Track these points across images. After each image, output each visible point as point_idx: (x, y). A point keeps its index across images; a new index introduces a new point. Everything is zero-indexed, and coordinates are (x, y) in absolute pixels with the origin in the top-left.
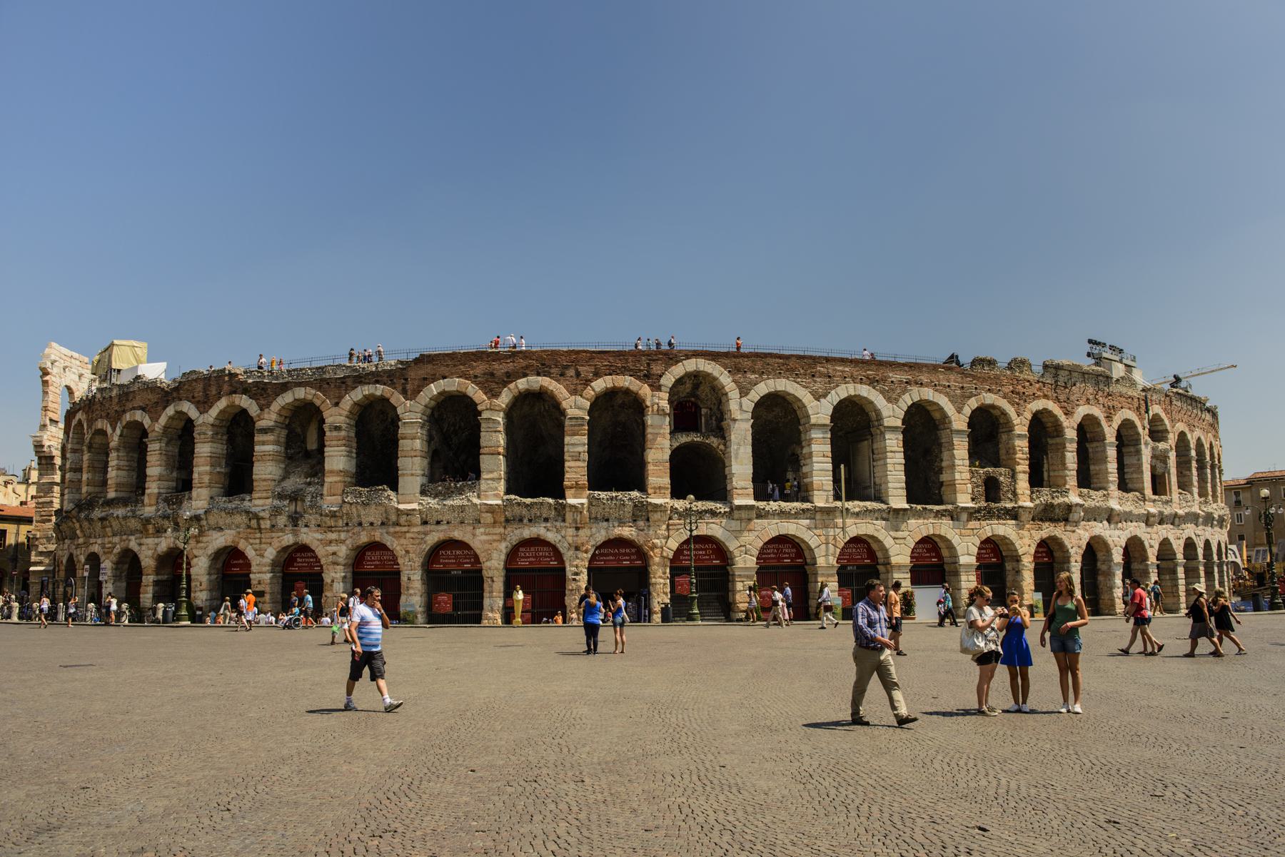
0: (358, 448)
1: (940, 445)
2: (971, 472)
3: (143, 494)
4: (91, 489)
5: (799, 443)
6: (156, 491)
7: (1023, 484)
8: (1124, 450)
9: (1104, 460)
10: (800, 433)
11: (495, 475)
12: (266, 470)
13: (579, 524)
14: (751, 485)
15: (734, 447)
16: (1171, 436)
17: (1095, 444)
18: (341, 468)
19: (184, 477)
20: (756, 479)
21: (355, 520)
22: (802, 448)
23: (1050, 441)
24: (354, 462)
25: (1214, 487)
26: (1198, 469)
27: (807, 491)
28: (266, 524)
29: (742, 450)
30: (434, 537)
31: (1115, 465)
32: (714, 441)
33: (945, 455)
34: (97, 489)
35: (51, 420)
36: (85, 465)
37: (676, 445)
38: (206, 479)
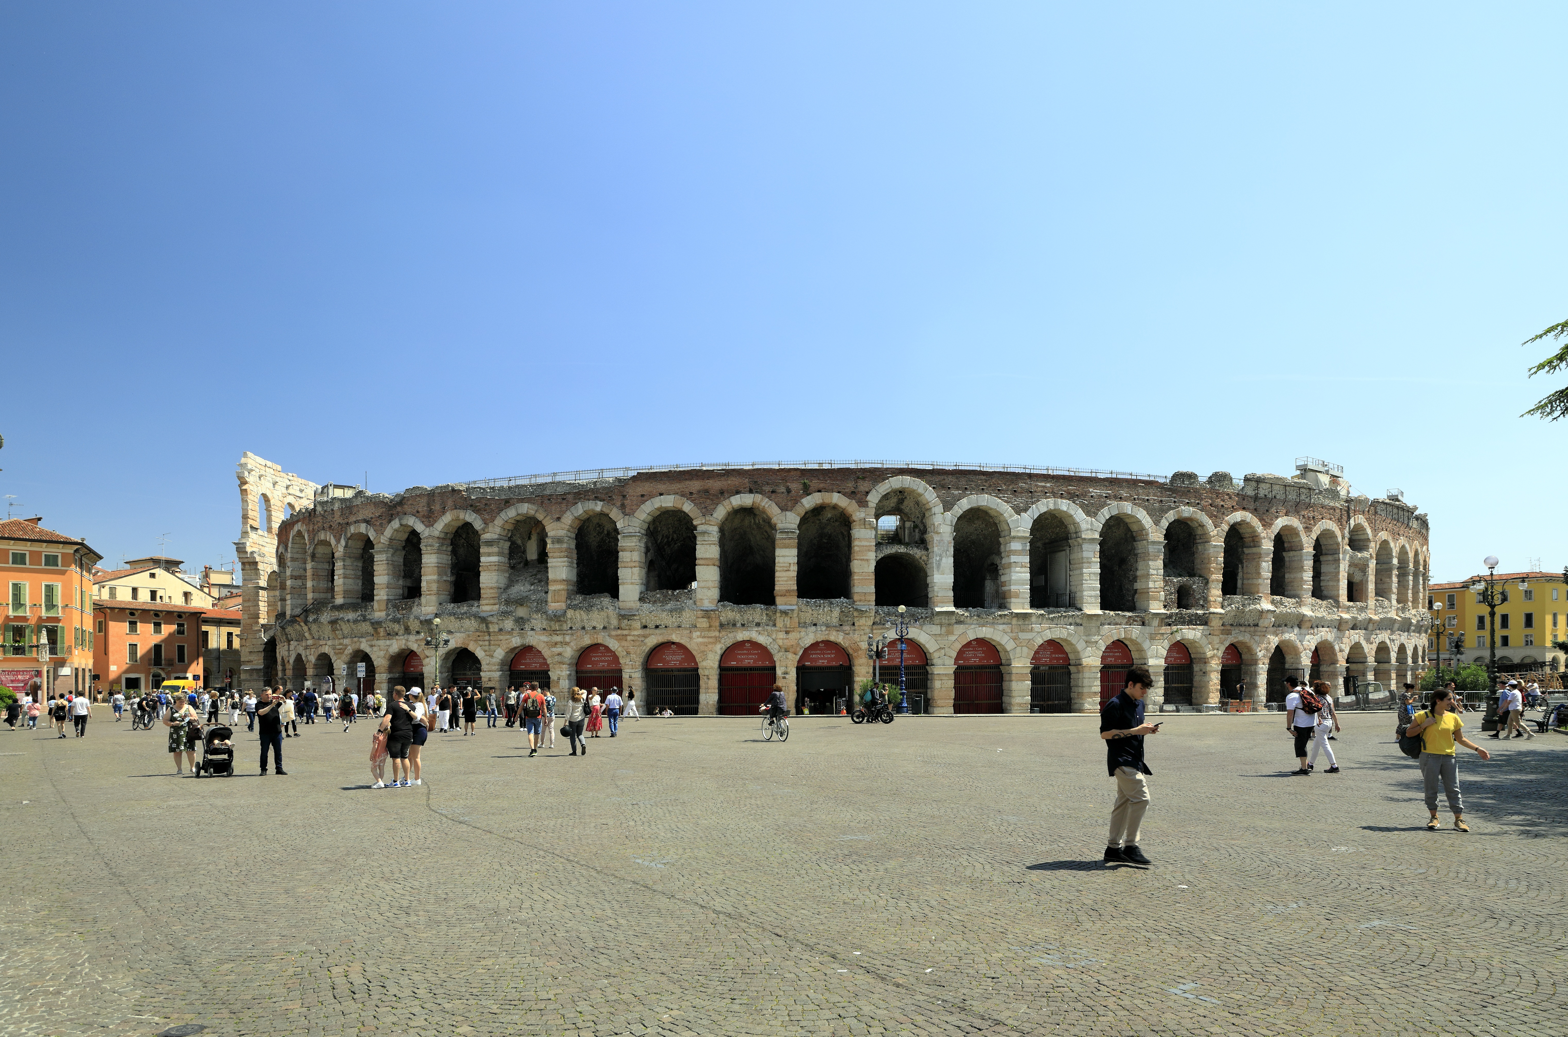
0: (578, 558)
1: (1136, 555)
2: (1165, 581)
3: (373, 600)
4: (317, 595)
5: (999, 553)
6: (385, 598)
7: (1216, 592)
8: (1322, 558)
9: (1301, 569)
10: (999, 544)
11: (710, 584)
12: (490, 578)
13: (788, 632)
14: (951, 594)
15: (935, 559)
16: (1372, 544)
17: (1291, 554)
18: (564, 576)
19: (409, 584)
20: (957, 587)
21: (578, 625)
22: (1002, 558)
23: (1246, 551)
24: (575, 571)
25: (1416, 593)
26: (1398, 576)
27: (1004, 598)
28: (494, 628)
29: (944, 560)
30: (653, 640)
31: (1311, 574)
32: (917, 553)
33: (1141, 565)
34: (322, 596)
35: (252, 527)
36: (309, 573)
37: (881, 556)
38: (434, 587)
